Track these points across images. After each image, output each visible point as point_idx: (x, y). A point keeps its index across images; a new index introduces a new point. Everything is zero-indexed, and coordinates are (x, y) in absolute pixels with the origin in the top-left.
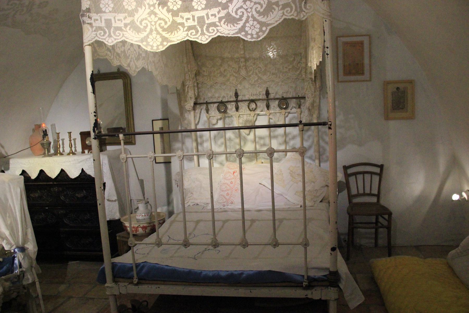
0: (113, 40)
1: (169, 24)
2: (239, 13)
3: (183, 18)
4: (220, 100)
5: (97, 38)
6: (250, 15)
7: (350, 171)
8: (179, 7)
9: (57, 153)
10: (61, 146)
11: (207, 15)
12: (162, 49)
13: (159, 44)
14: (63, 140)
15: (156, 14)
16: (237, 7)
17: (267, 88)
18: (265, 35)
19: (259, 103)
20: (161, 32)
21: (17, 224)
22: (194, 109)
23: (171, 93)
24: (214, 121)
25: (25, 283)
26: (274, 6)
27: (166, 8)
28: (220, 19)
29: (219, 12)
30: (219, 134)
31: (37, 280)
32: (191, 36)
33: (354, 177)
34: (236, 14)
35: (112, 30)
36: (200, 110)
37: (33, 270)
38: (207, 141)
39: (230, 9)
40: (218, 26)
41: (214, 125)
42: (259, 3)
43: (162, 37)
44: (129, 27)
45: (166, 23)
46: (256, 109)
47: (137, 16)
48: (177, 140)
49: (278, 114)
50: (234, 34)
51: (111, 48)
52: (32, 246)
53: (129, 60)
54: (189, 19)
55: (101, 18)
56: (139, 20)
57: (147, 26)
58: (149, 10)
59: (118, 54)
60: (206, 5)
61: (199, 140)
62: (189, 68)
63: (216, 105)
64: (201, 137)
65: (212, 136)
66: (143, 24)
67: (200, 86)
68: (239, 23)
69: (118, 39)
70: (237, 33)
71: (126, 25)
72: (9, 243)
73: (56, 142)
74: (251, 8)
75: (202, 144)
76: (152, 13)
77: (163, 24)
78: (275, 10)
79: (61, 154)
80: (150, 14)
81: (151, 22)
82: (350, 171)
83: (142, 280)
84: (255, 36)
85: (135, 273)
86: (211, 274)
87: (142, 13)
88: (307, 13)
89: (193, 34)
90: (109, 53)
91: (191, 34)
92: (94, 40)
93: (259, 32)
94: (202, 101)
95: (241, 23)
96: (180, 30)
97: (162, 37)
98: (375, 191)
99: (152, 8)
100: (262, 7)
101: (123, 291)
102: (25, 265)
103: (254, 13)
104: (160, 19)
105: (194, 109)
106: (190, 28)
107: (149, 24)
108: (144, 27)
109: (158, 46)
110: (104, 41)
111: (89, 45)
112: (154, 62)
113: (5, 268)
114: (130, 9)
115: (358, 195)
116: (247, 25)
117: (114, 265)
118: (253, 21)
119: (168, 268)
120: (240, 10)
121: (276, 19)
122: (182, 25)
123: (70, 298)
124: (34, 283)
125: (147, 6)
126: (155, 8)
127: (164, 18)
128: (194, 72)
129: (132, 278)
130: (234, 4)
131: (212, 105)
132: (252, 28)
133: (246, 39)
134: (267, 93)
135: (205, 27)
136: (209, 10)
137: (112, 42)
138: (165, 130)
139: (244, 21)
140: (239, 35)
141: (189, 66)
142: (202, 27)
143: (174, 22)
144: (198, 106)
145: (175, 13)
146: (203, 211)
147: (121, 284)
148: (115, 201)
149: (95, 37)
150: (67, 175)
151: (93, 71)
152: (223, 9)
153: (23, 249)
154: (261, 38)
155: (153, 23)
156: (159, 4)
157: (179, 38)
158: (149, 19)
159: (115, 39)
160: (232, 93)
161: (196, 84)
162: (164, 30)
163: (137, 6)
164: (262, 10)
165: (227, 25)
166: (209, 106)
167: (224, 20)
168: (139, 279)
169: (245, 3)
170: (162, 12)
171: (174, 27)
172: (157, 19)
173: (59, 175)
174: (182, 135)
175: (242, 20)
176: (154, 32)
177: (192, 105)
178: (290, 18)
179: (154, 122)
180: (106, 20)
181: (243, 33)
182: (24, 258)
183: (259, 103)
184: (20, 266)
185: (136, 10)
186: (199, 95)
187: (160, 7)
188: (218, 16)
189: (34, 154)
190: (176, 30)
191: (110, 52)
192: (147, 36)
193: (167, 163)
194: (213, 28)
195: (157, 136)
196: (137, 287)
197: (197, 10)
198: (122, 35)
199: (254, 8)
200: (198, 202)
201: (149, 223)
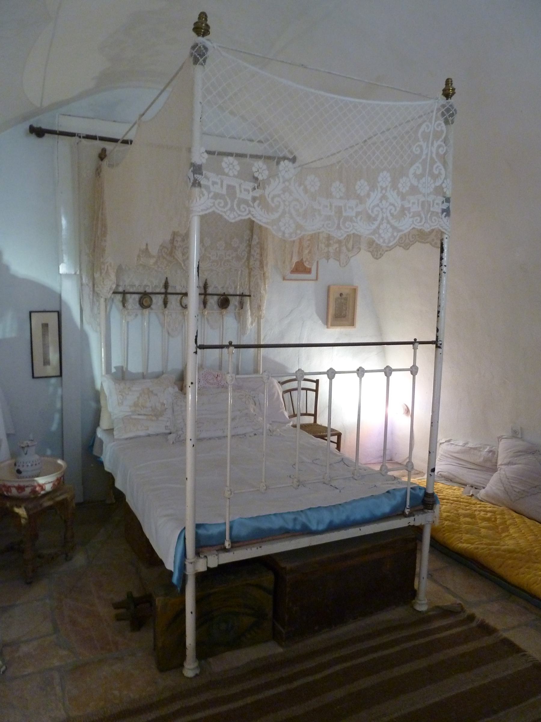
0: (237, 216)
4: (141, 290)
6: (385, 215)
17: (206, 280)
26: (406, 212)
28: (358, 214)
29: (357, 205)
34: (372, 212)
35: (236, 202)
42: (394, 206)
44: (257, 202)
54: (327, 207)
55: (222, 182)
56: (271, 196)
68: (374, 222)
69: (242, 216)
71: (254, 199)
78: (406, 216)
80: (284, 190)
81: (284, 201)
103: (389, 215)
110: (223, 214)
137: (235, 218)
139: (378, 222)
149: (211, 207)
158: (282, 196)
159: (239, 215)
169: (381, 202)
175: (376, 220)
179: (33, 314)
180: (229, 187)
181: (377, 235)
198: (247, 212)
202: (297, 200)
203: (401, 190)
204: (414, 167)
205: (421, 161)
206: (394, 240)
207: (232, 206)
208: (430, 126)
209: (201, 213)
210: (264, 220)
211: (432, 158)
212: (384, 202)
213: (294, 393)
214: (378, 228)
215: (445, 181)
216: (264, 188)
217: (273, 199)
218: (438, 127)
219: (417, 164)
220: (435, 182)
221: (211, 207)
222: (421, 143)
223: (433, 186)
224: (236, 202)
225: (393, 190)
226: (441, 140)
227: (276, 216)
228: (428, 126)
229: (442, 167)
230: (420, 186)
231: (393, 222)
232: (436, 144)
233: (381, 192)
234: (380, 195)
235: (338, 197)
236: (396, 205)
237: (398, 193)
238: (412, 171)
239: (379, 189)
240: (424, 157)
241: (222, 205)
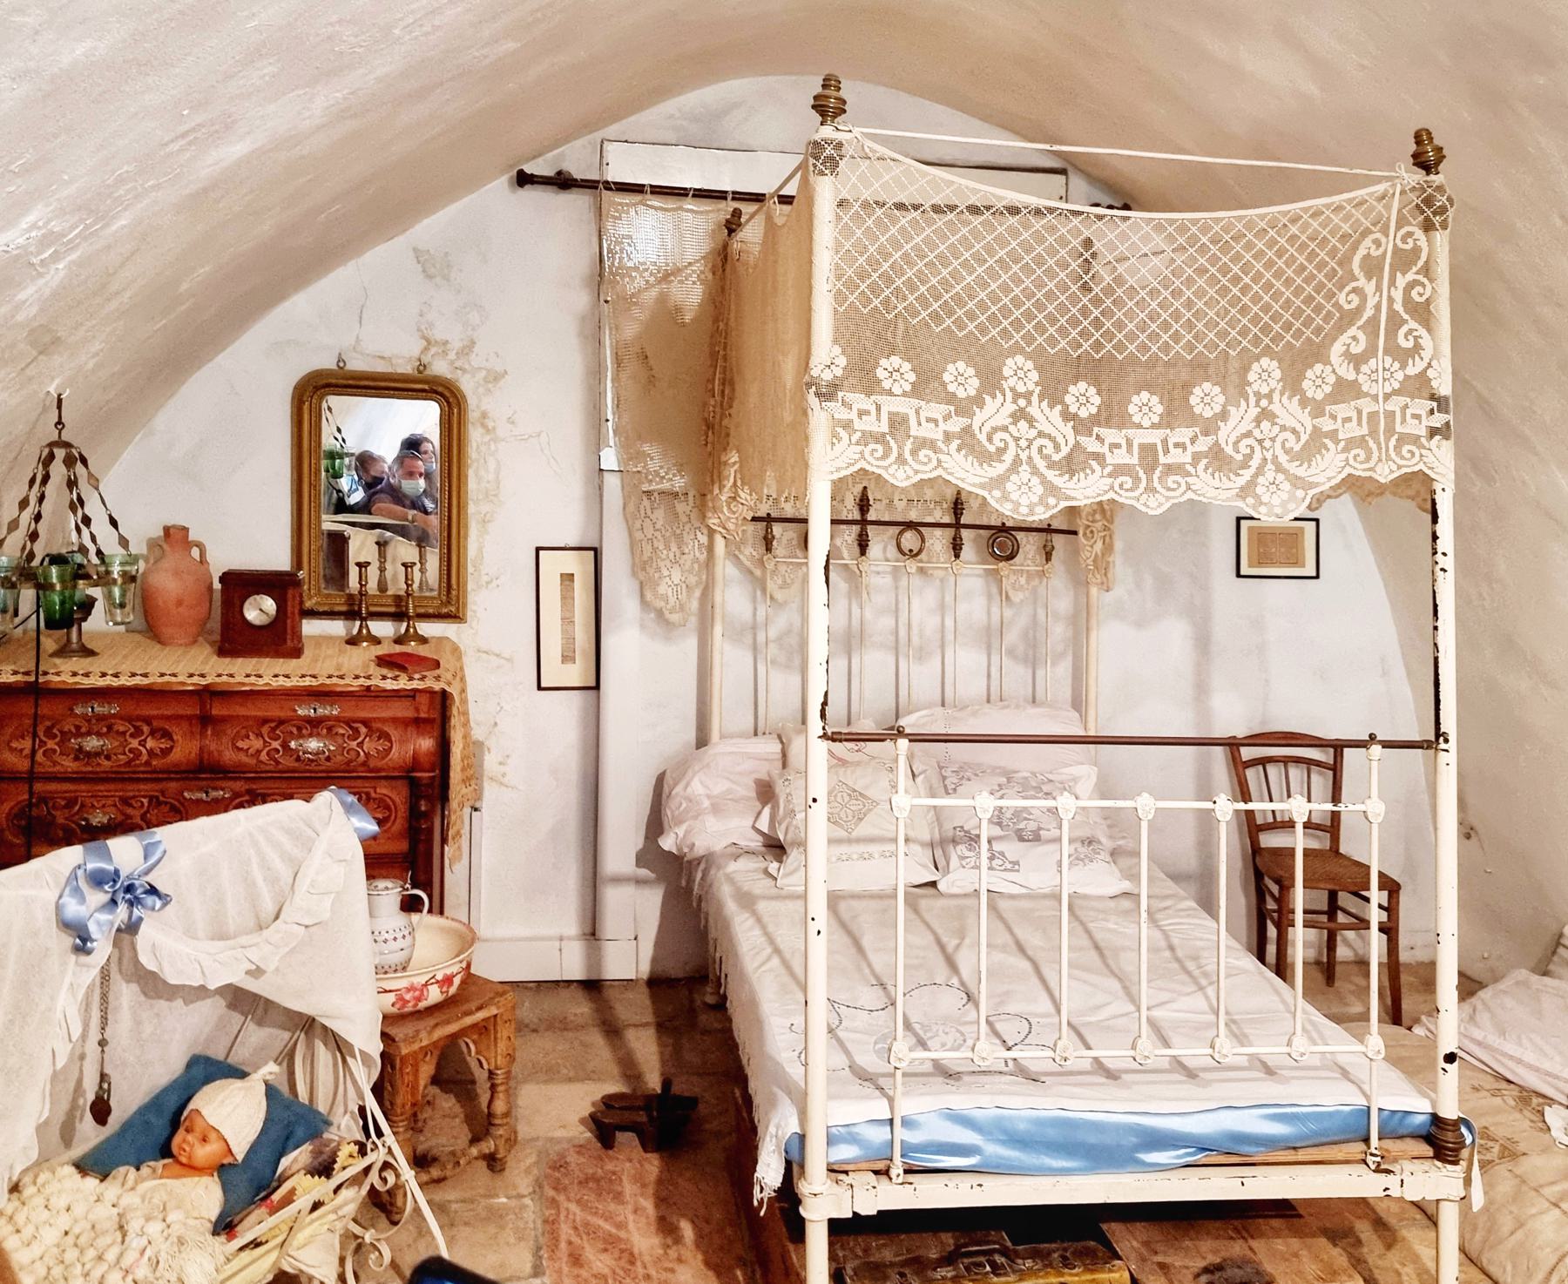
0: (910, 473)
1: (1065, 450)
6: (1269, 456)
8: (1094, 410)
11: (1165, 441)
13: (1035, 499)
15: (1031, 422)
20: (1043, 470)
26: (1327, 441)
27: (1059, 407)
39: (1222, 435)
40: (1189, 474)
42: (1294, 431)
44: (955, 443)
45: (1057, 448)
54: (1118, 446)
55: (878, 408)
56: (987, 428)
71: (948, 437)
74: (1273, 440)
76: (1020, 415)
77: (1049, 450)
81: (1017, 439)
87: (996, 411)
88: (1399, 467)
91: (1121, 486)
95: (1247, 474)
96: (1093, 472)
97: (1044, 482)
99: (1022, 403)
100: (1298, 439)
104: (1041, 434)
106: (1120, 470)
107: (1012, 444)
108: (998, 449)
109: (1031, 507)
114: (961, 394)
116: (1261, 480)
121: (1330, 473)
122: (1099, 458)
125: (1009, 395)
126: (1029, 403)
127: (1054, 433)
130: (1232, 422)
135: (1157, 473)
137: (908, 477)
139: (1252, 470)
142: (1150, 470)
145: (1083, 426)
149: (856, 461)
155: (1023, 443)
156: (1041, 398)
157: (1089, 492)
158: (1012, 428)
159: (916, 472)
162: (1051, 465)
163: (980, 393)
164: (1297, 448)
170: (1048, 418)
172: (1033, 433)
176: (1025, 467)
178: (1367, 474)
185: (978, 401)
187: (1045, 404)
190: (1083, 470)
197: (1139, 426)
199: (1279, 440)
202: (1049, 437)
203: (1309, 394)
204: (1345, 338)
205: (1360, 323)
208: (1384, 240)
209: (836, 476)
211: (1393, 314)
212: (1265, 425)
214: (1252, 483)
215: (1434, 363)
216: (971, 415)
217: (990, 439)
218: (1404, 240)
219: (1353, 331)
220: (1403, 367)
221: (856, 461)
222: (1362, 282)
223: (1400, 376)
226: (1415, 269)
227: (1000, 468)
228: (1377, 243)
229: (1422, 332)
230: (1361, 378)
231: (1293, 468)
232: (1401, 281)
233: (1257, 405)
234: (1254, 412)
235: (1146, 423)
236: (1299, 428)
237: (1304, 402)
238: (1337, 349)
239: (1252, 400)
240: (1369, 313)
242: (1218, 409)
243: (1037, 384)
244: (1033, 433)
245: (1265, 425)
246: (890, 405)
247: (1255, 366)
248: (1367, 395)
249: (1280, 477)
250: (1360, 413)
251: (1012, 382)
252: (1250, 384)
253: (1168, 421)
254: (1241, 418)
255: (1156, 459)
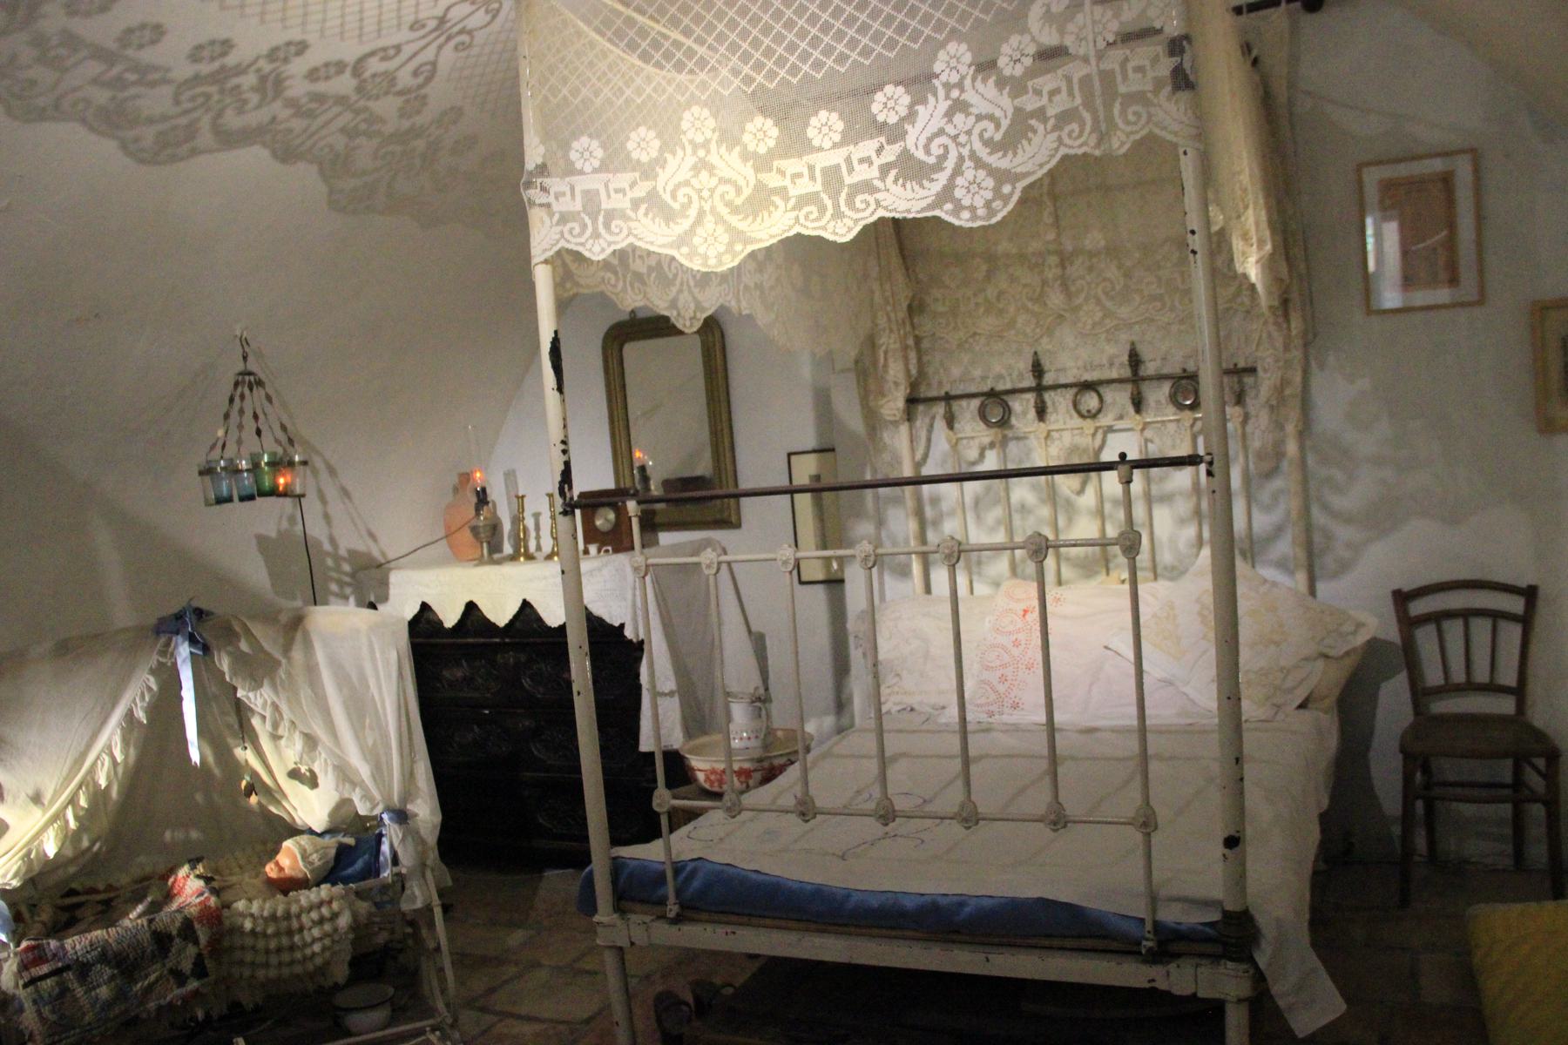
1: (747, 192)
2: (936, 150)
3: (782, 173)
5: (562, 244)
6: (965, 152)
7: (1418, 608)
8: (772, 143)
9: (521, 553)
10: (533, 534)
11: (848, 160)
12: (730, 263)
14: (537, 516)
15: (711, 169)
16: (927, 133)
17: (1133, 344)
18: (1010, 207)
19: (1109, 394)
20: (728, 218)
21: (388, 746)
22: (910, 416)
23: (842, 371)
24: (973, 454)
25: (405, 906)
26: (1033, 122)
27: (738, 149)
29: (879, 151)
30: (988, 490)
31: (436, 901)
32: (811, 225)
33: (1430, 629)
34: (928, 152)
35: (601, 219)
36: (927, 420)
37: (429, 875)
38: (952, 513)
39: (910, 141)
40: (877, 190)
41: (974, 463)
42: (991, 117)
43: (730, 229)
44: (643, 207)
45: (739, 191)
46: (1099, 411)
47: (663, 176)
48: (859, 514)
49: (1172, 427)
50: (923, 210)
51: (615, 262)
52: (426, 811)
53: (674, 290)
54: (799, 175)
55: (572, 189)
56: (670, 188)
57: (690, 202)
58: (694, 159)
59: (638, 277)
60: (844, 134)
61: (929, 512)
62: (888, 294)
63: (976, 403)
64: (935, 501)
65: (968, 499)
66: (682, 199)
67: (925, 344)
68: (935, 176)
70: (931, 207)
71: (636, 204)
72: (367, 796)
73: (518, 519)
74: (969, 133)
75: (937, 523)
76: (702, 166)
77: (731, 195)
78: (1035, 132)
79: (530, 557)
80: (696, 169)
81: (699, 191)
82: (1418, 608)
83: (691, 910)
84: (981, 212)
85: (670, 889)
86: (874, 903)
87: (677, 168)
89: (812, 217)
90: (609, 275)
91: (806, 217)
92: (556, 249)
93: (993, 200)
94: (933, 393)
95: (942, 178)
97: (730, 229)
98: (1509, 677)
99: (701, 153)
100: (998, 126)
101: (639, 935)
102: (407, 860)
104: (723, 181)
105: (910, 416)
106: (803, 201)
109: (719, 256)
111: (546, 262)
112: (759, 286)
113: (359, 864)
114: (644, 158)
115: (1449, 689)
116: (960, 181)
117: (617, 866)
118: (976, 168)
119: (761, 878)
120: (937, 141)
121: (1040, 159)
122: (782, 192)
123: (536, 965)
124: (428, 909)
126: (708, 152)
128: (905, 305)
129: (662, 902)
130: (920, 124)
131: (964, 403)
132: (974, 188)
133: (956, 222)
134: (1135, 360)
136: (851, 147)
137: (603, 250)
138: (827, 480)
139: (948, 172)
140: (937, 213)
141: (887, 287)
142: (835, 197)
143: (760, 187)
144: (921, 408)
145: (762, 163)
146: (925, 727)
147: (633, 917)
148: (671, 694)
150: (540, 619)
151: (556, 332)
152: (889, 142)
153: (402, 816)
154: (999, 217)
155: (706, 194)
156: (720, 142)
159: (610, 244)
160: (1024, 365)
161: (911, 342)
162: (735, 210)
163: (661, 150)
164: (998, 137)
165: (904, 185)
166: (955, 405)
167: (893, 173)
168: (682, 906)
169: (950, 121)
171: (760, 200)
172: (714, 181)
173: (516, 617)
174: (877, 498)
175: (942, 169)
177: (901, 404)
178: (1080, 152)
179: (793, 458)
180: (586, 193)
181: (949, 206)
182: (403, 840)
183: (1109, 394)
184: (395, 861)
185: (660, 162)
186: (922, 373)
188: (877, 162)
189: (458, 556)
190: (767, 208)
191: (616, 273)
192: (692, 231)
193: (835, 583)
194: (866, 196)
195: (804, 501)
196: (674, 929)
197: (820, 149)
198: (625, 232)
199: (976, 131)
200: (913, 701)
201: (760, 760)
206: (1005, 205)
207: (595, 230)
210: (661, 241)
213: (1454, 629)
216: (655, 177)
217: (674, 197)
224: (601, 219)
225: (984, 81)
227: (686, 224)
233: (947, 97)
235: (827, 144)
239: (941, 92)
241: (577, 230)
242: (903, 111)
243: (714, 131)
244: (714, 181)
245: (959, 118)
246: (582, 184)
247: (942, 55)
248: (1075, 57)
249: (982, 174)
250: (1069, 79)
251: (690, 135)
252: (937, 76)
253: (849, 138)
254: (931, 114)
255: (841, 181)
